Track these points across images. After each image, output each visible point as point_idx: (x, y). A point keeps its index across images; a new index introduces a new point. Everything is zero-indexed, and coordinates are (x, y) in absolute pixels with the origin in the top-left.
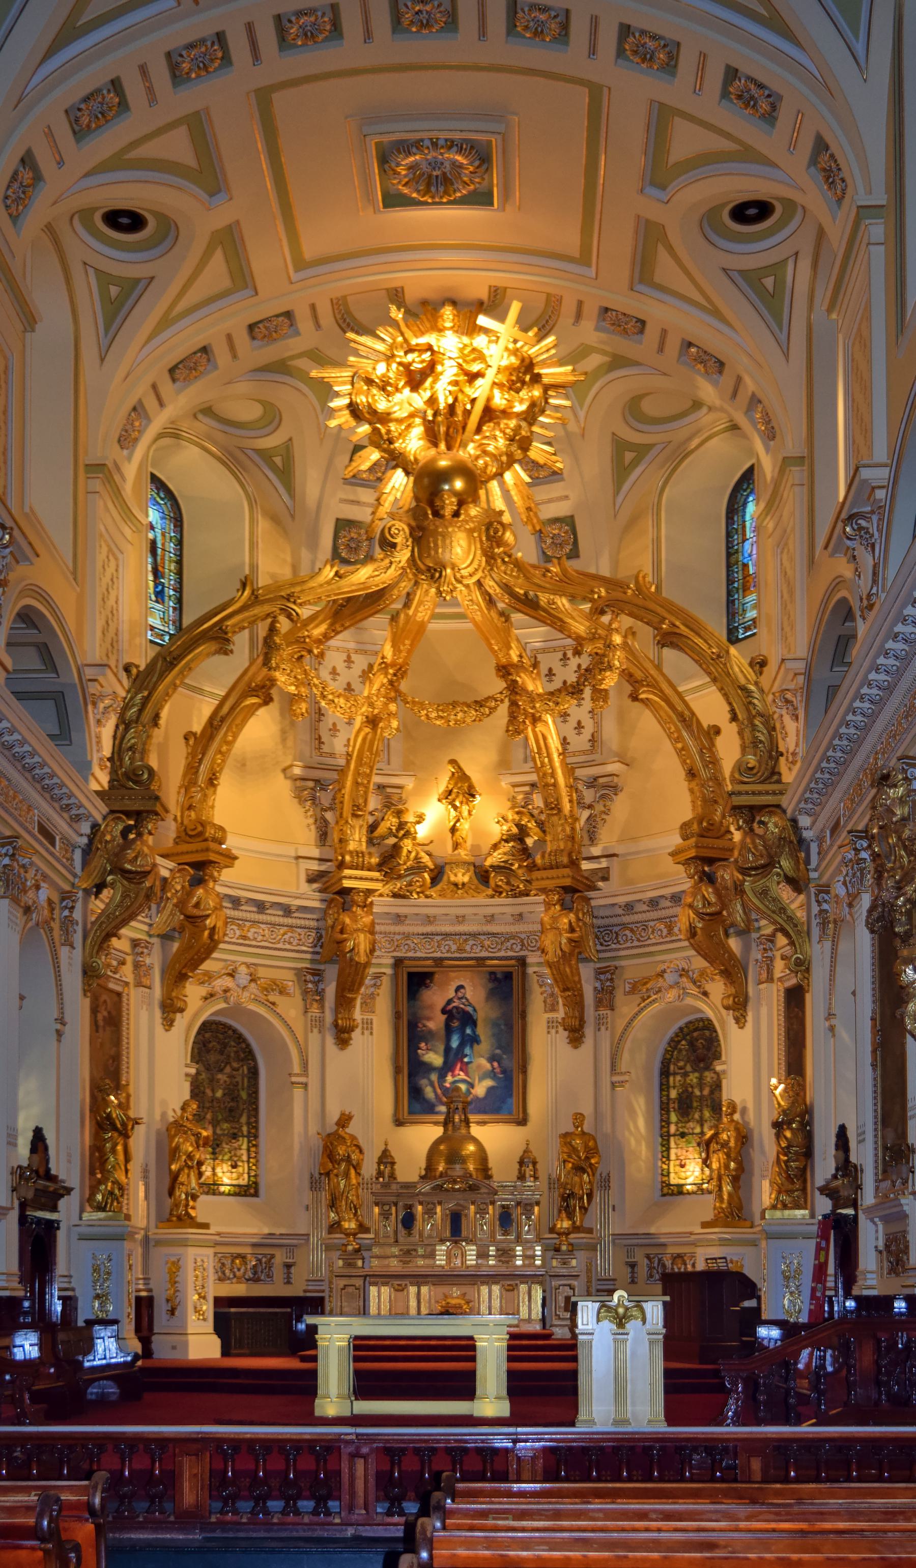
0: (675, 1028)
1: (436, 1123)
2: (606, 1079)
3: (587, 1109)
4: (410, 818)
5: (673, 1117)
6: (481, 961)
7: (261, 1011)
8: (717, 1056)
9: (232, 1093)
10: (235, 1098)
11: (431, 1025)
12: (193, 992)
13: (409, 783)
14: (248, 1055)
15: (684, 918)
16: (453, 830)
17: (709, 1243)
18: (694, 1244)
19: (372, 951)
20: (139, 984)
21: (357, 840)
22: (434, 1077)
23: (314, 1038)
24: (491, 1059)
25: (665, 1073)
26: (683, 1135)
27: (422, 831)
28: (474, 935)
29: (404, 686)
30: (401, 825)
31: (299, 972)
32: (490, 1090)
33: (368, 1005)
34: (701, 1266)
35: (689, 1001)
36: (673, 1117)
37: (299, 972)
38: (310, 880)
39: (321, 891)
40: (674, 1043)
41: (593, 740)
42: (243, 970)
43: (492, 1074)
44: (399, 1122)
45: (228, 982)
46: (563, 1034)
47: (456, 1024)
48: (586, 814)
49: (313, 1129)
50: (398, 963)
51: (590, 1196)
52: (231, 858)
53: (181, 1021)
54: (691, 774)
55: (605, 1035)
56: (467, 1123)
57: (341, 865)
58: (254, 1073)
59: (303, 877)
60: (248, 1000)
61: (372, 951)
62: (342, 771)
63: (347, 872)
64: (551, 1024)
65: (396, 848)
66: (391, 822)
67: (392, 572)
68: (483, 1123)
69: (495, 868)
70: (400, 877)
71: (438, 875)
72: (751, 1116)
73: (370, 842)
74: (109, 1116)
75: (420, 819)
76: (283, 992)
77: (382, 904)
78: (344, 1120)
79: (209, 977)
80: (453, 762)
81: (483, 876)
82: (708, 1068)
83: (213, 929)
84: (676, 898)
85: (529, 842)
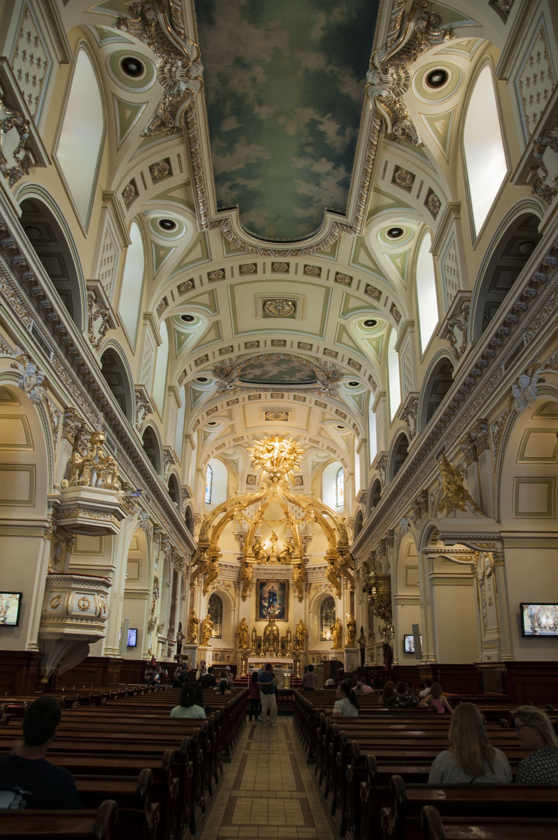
0: (324, 598)
1: (266, 621)
2: (308, 611)
3: (303, 619)
4: (262, 545)
5: (324, 621)
6: (278, 580)
7: (225, 592)
8: (335, 606)
9: (216, 612)
10: (217, 613)
11: (265, 596)
12: (210, 587)
13: (262, 536)
14: (220, 602)
15: (327, 573)
16: (272, 548)
17: (332, 653)
18: (328, 653)
19: (252, 578)
20: (198, 585)
21: (250, 551)
22: (266, 609)
23: (237, 598)
24: (280, 605)
25: (322, 609)
26: (326, 625)
27: (265, 548)
28: (276, 574)
29: (262, 516)
30: (260, 547)
31: (234, 582)
32: (279, 613)
33: (250, 591)
34: (330, 659)
35: (328, 592)
36: (324, 621)
37: (234, 582)
38: (238, 559)
39: (240, 562)
40: (324, 602)
41: (306, 528)
42: (221, 581)
43: (280, 609)
44: (257, 620)
45: (218, 584)
46: (297, 599)
47: (271, 596)
48: (304, 545)
49: (236, 622)
50: (258, 580)
51: (303, 641)
52: (221, 555)
53: (207, 594)
54: (329, 540)
55: (307, 600)
56: (274, 621)
57: (246, 556)
58: (222, 607)
59: (236, 559)
60: (222, 588)
61: (252, 578)
62: (247, 534)
63: (247, 558)
64: (295, 596)
65: (258, 552)
66: (258, 546)
67: (263, 494)
68: (277, 621)
69: (283, 558)
70: (259, 559)
71: (268, 559)
72: (342, 622)
73: (253, 550)
74: (194, 619)
75: (264, 545)
76: (230, 586)
77: (255, 566)
78: (244, 620)
79: (214, 583)
80: (273, 532)
81: (279, 559)
82: (332, 609)
83: (217, 573)
84: (325, 567)
85: (290, 551)
